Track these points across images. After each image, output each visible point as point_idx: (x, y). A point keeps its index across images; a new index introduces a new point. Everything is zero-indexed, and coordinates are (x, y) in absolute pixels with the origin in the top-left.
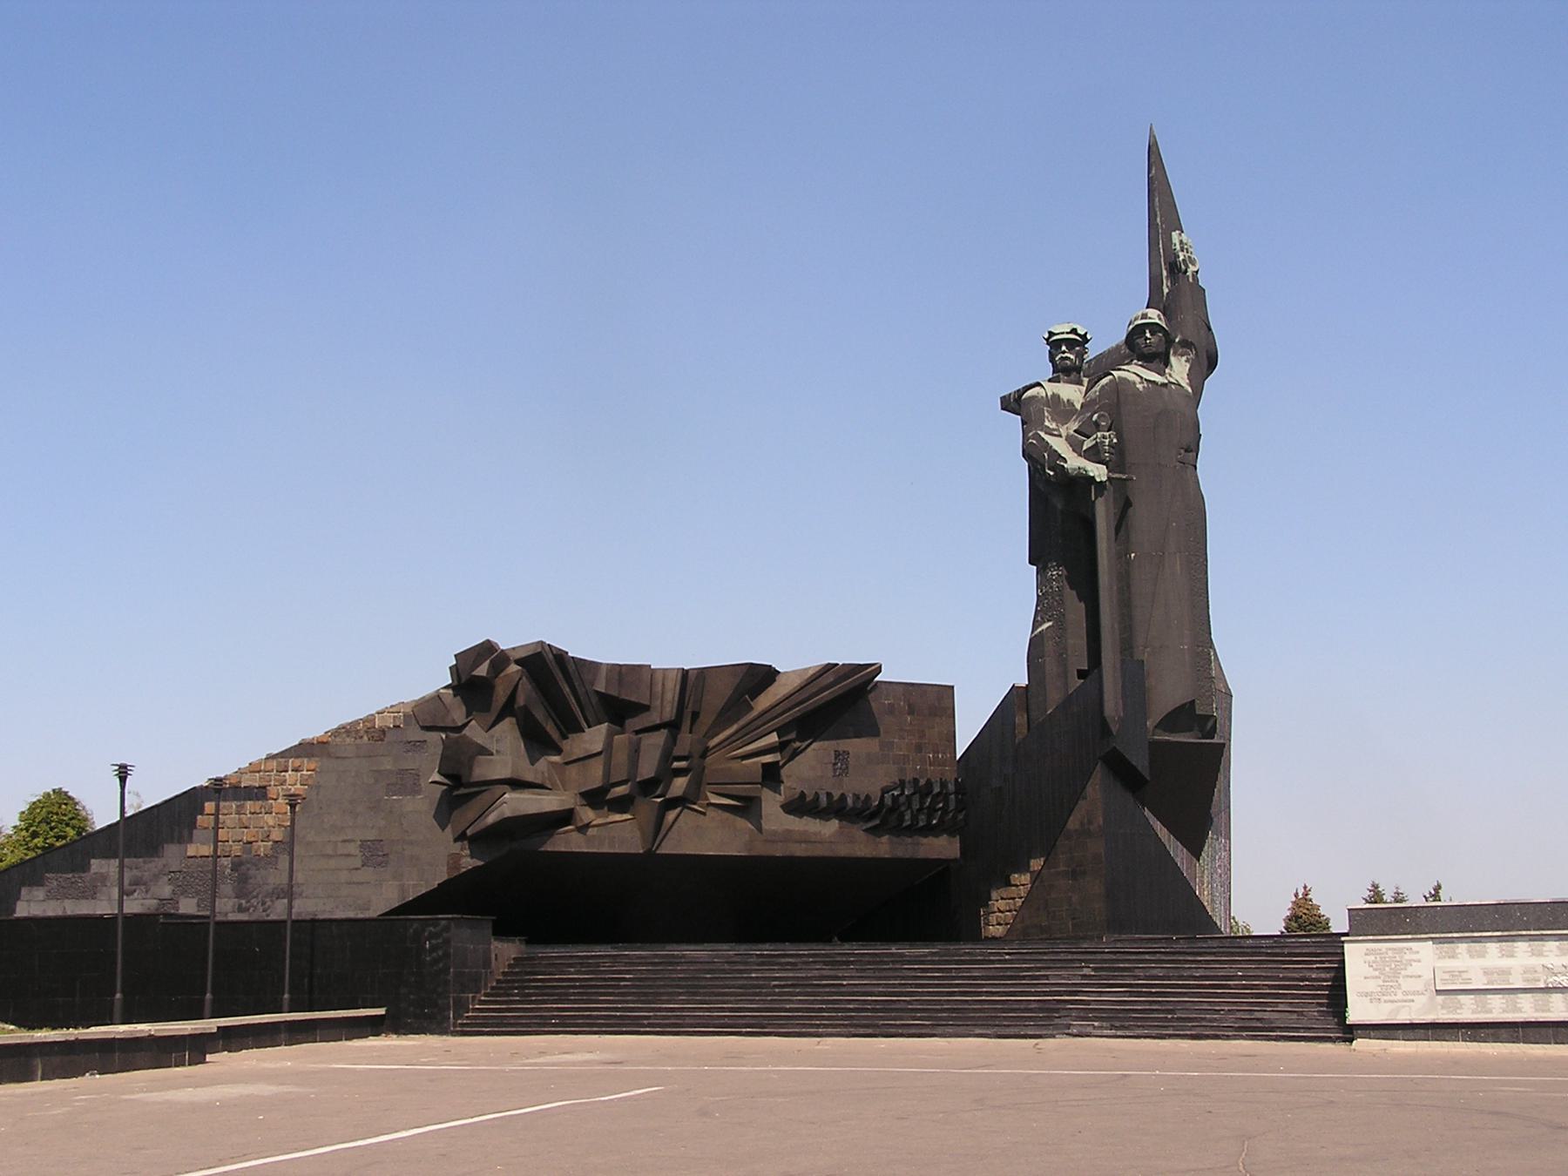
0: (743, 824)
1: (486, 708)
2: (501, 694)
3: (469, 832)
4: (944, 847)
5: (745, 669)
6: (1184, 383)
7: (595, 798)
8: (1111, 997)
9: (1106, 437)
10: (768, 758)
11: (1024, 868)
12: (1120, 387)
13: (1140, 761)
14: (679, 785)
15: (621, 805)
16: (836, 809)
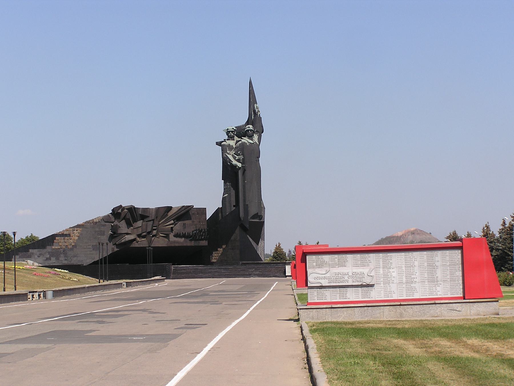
0: (166, 240)
1: (119, 218)
2: (123, 215)
4: (204, 243)
7: (139, 236)
8: (257, 273)
9: (241, 157)
10: (171, 226)
11: (221, 247)
12: (244, 144)
13: (247, 226)
14: (155, 232)
15: (144, 237)
16: (184, 236)
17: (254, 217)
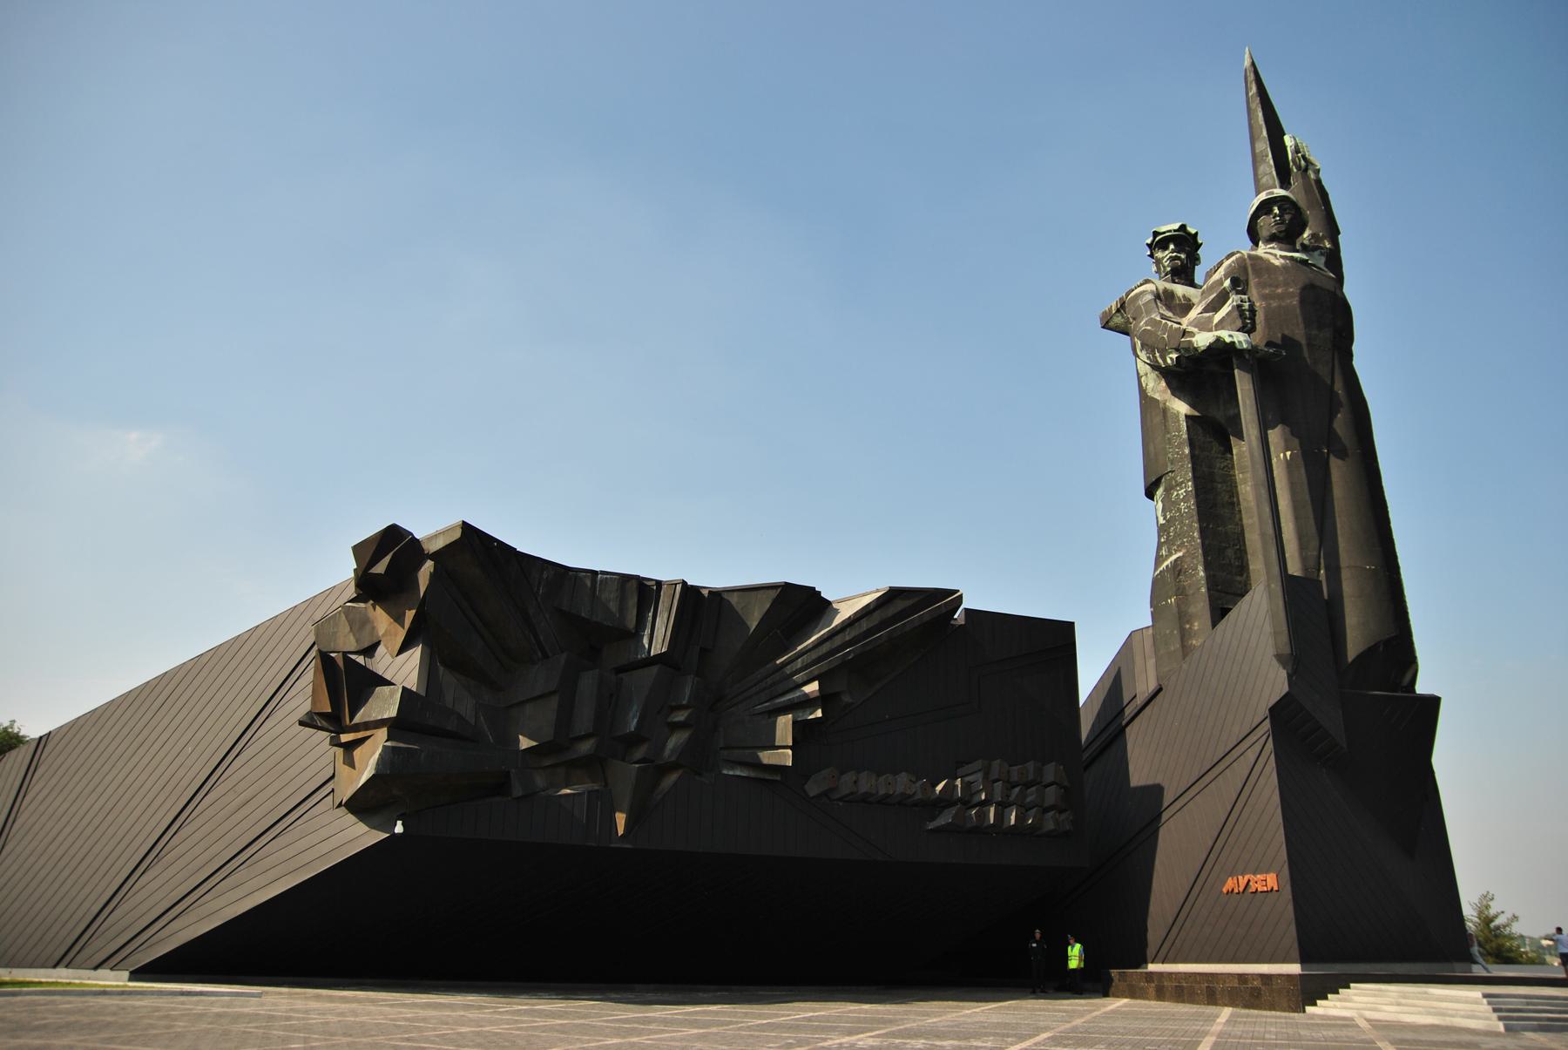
5: (774, 594)
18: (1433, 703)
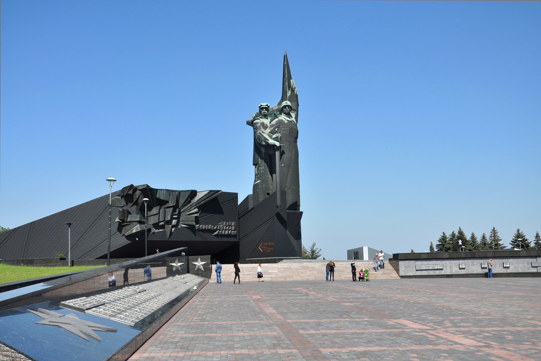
1: (131, 202)
3: (126, 234)
6: (295, 120)
9: (279, 135)
10: (196, 215)
17: (290, 208)
18: (302, 213)
